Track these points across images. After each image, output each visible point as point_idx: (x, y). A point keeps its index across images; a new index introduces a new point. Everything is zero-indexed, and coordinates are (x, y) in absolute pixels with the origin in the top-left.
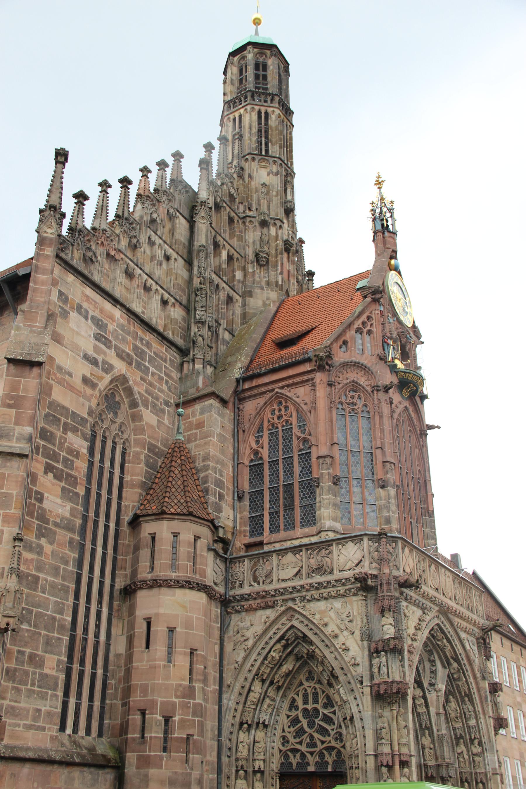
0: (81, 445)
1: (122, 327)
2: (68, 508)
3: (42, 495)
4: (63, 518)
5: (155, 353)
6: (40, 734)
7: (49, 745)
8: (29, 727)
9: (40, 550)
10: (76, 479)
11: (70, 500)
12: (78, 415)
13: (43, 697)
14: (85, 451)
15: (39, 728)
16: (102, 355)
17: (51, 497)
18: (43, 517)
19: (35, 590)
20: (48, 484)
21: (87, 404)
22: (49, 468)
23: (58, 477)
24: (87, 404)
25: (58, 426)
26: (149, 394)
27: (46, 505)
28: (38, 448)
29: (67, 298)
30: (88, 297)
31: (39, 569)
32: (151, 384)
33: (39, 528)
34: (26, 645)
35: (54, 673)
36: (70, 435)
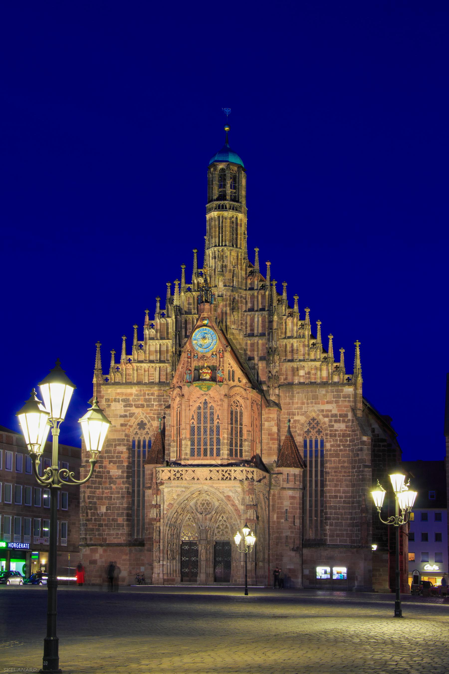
0: (123, 449)
1: (137, 395)
2: (120, 471)
3: (109, 471)
4: (119, 475)
5: (156, 396)
6: (119, 540)
7: (123, 542)
8: (115, 538)
9: (111, 488)
10: (122, 461)
11: (121, 469)
12: (120, 439)
13: (119, 529)
14: (125, 450)
15: (118, 538)
16: (129, 412)
17: (113, 471)
18: (110, 478)
19: (111, 500)
20: (111, 467)
21: (124, 433)
22: (110, 462)
23: (115, 463)
24: (124, 433)
25: (112, 447)
26: (155, 415)
27: (111, 474)
28: (105, 457)
29: (109, 399)
30: (118, 394)
31: (111, 494)
32: (155, 410)
33: (110, 482)
34: (110, 516)
35: (122, 522)
36: (118, 447)
